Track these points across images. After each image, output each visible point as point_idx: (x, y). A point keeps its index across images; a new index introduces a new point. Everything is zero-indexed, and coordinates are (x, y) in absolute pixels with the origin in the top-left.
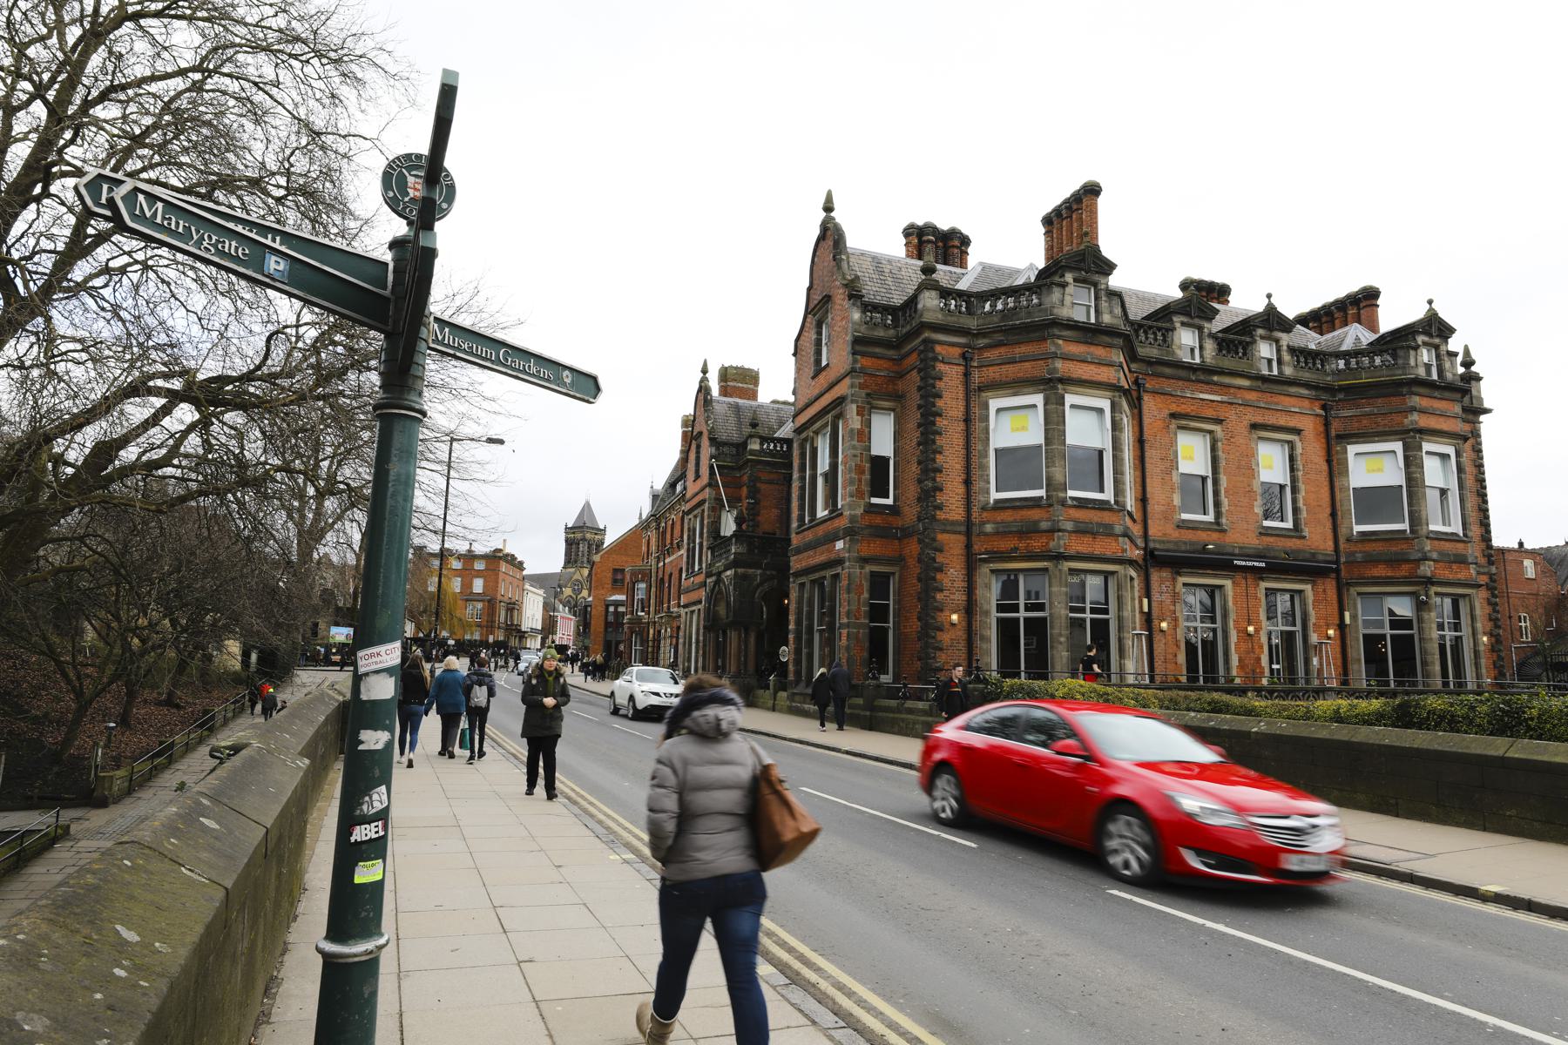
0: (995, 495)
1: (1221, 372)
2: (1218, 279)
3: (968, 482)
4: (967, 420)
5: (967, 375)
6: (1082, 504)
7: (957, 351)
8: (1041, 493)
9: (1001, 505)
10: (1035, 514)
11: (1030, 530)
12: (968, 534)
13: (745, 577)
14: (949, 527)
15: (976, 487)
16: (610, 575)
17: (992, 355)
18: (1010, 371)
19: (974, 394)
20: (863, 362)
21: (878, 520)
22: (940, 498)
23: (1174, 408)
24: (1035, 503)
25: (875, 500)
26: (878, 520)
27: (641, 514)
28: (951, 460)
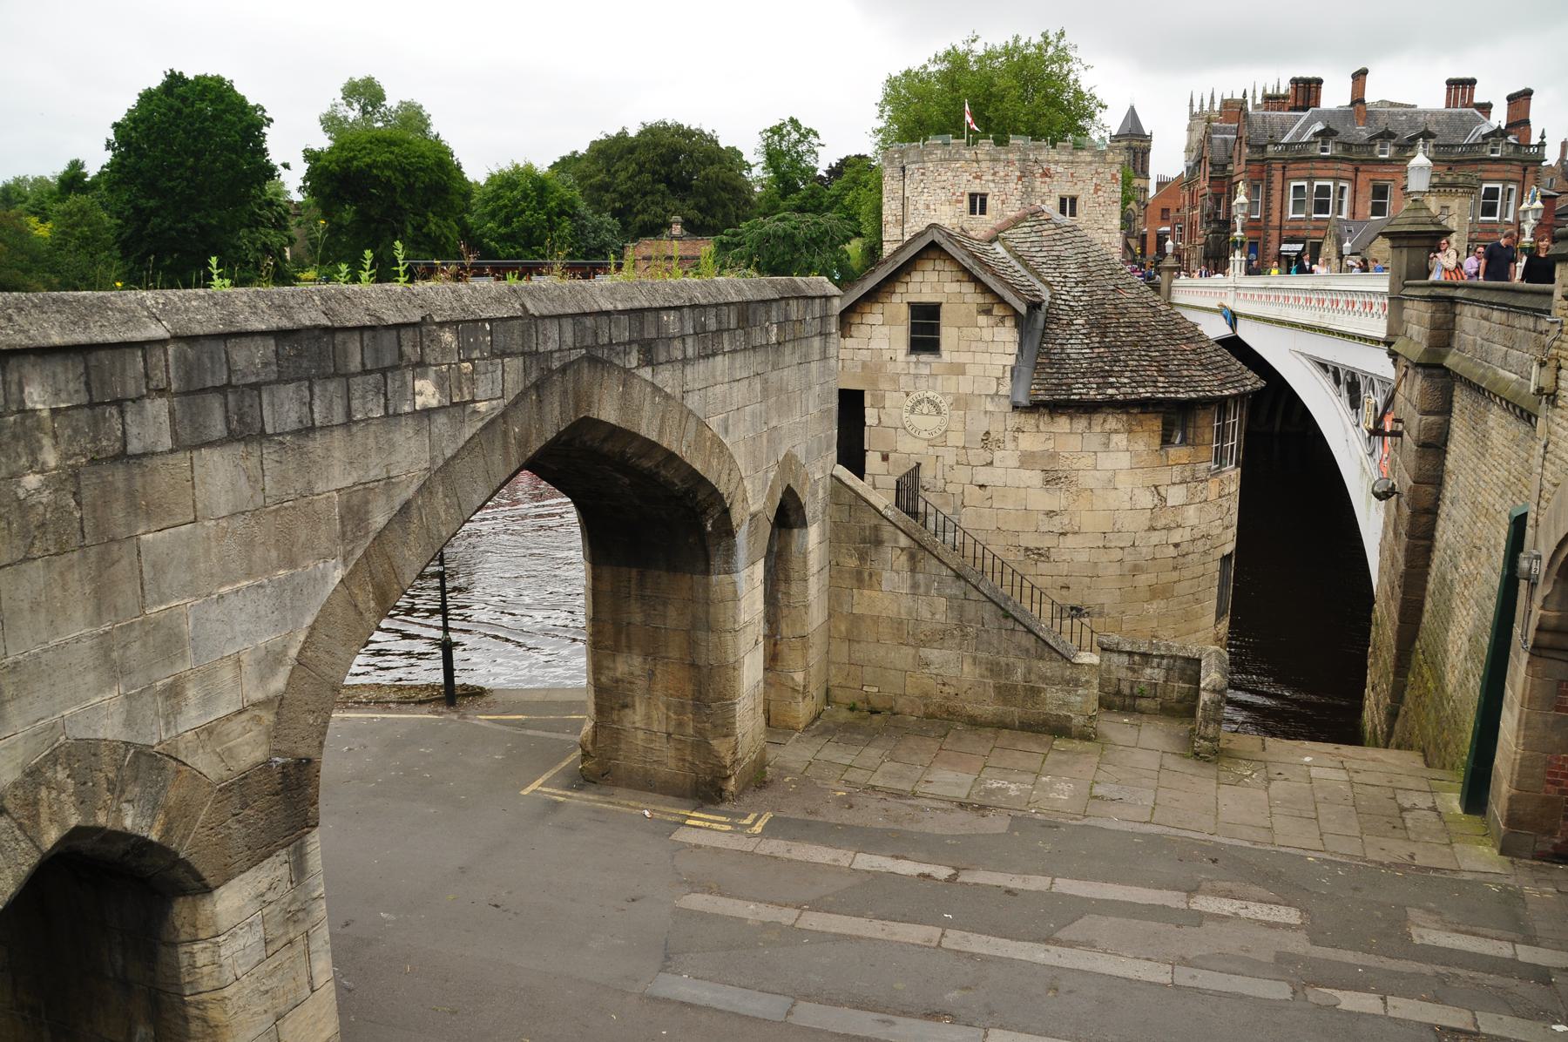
0: (1291, 215)
1: (1396, 160)
2: (1469, 76)
3: (1281, 212)
4: (1283, 190)
5: (1284, 174)
6: (1317, 219)
7: (1280, 165)
8: (1303, 216)
9: (1293, 220)
10: (1302, 223)
11: (1299, 229)
12: (1280, 229)
13: (1217, 237)
14: (1274, 228)
15: (1285, 213)
16: (1159, 213)
17: (1292, 166)
18: (1298, 173)
19: (1285, 179)
20: (1251, 167)
21: (1253, 224)
22: (1271, 218)
23: (1372, 177)
24: (1301, 220)
25: (1253, 217)
26: (1253, 224)
27: (1191, 105)
28: (1276, 205)
